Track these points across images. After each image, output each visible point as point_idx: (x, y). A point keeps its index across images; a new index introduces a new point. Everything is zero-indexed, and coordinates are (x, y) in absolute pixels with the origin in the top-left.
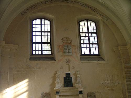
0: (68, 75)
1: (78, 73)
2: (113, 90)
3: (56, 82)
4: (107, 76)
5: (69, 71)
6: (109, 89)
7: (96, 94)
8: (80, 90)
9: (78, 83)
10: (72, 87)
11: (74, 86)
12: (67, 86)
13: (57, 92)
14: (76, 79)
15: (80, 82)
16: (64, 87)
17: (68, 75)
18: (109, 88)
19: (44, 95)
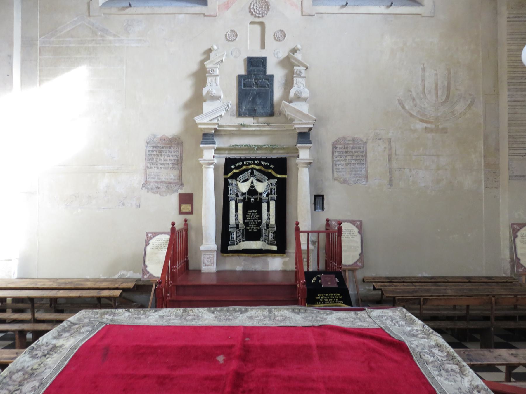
0: (256, 64)
1: (298, 56)
2: (444, 131)
3: (205, 91)
4: (424, 70)
5: (263, 46)
6: (429, 126)
7: (369, 146)
8: (304, 126)
9: (298, 98)
10: (272, 115)
11: (280, 113)
12: (252, 113)
13: (205, 135)
14: (289, 84)
15: (306, 93)
16: (240, 114)
17: (256, 64)
18: (426, 122)
19: (156, 147)
